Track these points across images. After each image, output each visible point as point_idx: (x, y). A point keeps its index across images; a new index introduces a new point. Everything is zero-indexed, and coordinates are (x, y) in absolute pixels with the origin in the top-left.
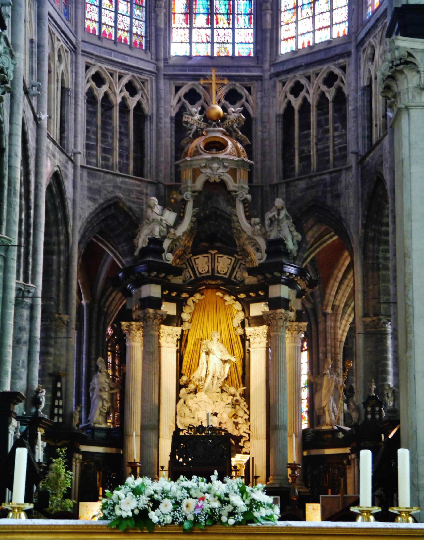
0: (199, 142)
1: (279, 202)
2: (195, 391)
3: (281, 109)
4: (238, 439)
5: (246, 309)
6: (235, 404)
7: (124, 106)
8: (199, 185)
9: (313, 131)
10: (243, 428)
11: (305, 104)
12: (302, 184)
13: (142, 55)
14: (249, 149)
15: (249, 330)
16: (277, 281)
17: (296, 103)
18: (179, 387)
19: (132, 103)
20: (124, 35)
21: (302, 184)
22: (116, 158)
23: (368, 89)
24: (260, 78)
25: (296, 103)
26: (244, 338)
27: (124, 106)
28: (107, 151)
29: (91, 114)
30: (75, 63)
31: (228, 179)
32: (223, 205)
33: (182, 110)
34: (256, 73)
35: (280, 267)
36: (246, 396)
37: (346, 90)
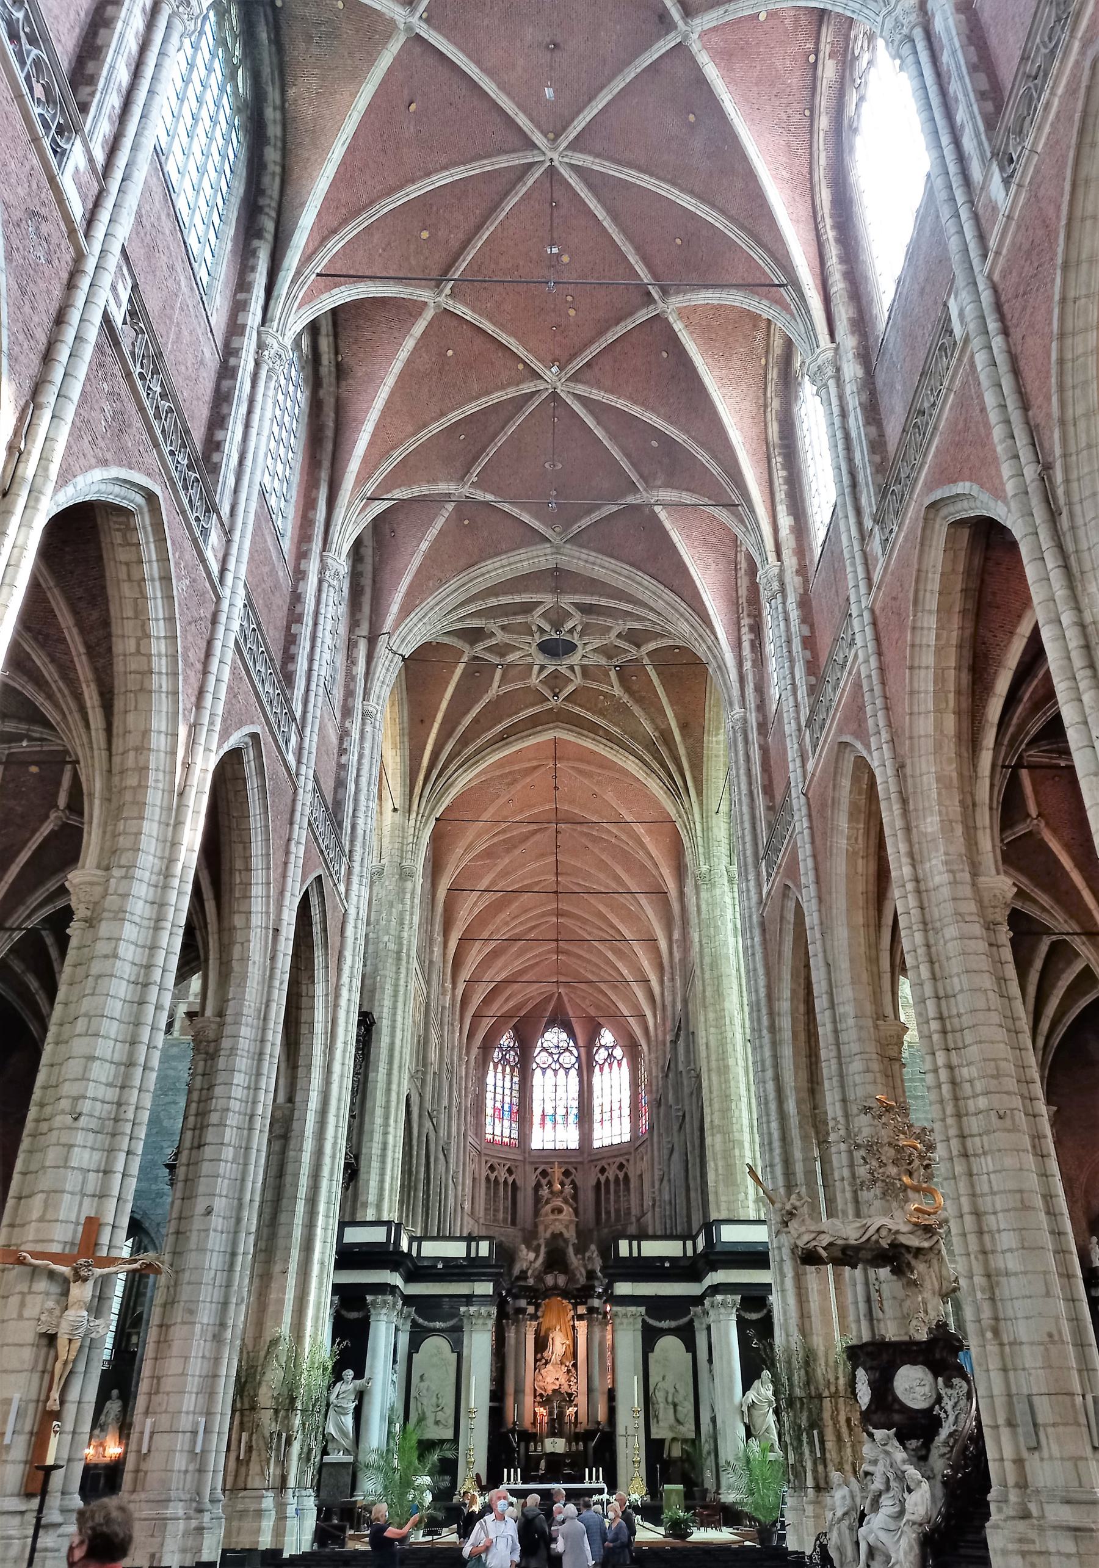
0: (548, 1207)
1: (593, 1247)
2: (546, 1363)
3: (594, 1182)
4: (570, 1395)
5: (575, 1309)
6: (569, 1371)
7: (506, 1182)
8: (548, 1235)
9: (612, 1197)
10: (574, 1388)
11: (607, 1180)
12: (606, 1230)
13: (516, 1151)
14: (576, 1212)
15: (577, 1323)
16: (592, 1297)
17: (603, 1179)
18: (536, 1361)
19: (510, 1180)
20: (506, 1140)
21: (606, 1230)
22: (501, 1215)
23: (641, 1176)
24: (581, 1163)
25: (603, 1179)
26: (574, 1327)
27: (506, 1182)
28: (496, 1210)
29: (488, 1188)
30: (480, 1162)
31: (564, 1231)
32: (561, 1243)
33: (538, 1186)
34: (579, 1159)
35: (593, 1287)
36: (575, 1365)
37: (631, 1175)
